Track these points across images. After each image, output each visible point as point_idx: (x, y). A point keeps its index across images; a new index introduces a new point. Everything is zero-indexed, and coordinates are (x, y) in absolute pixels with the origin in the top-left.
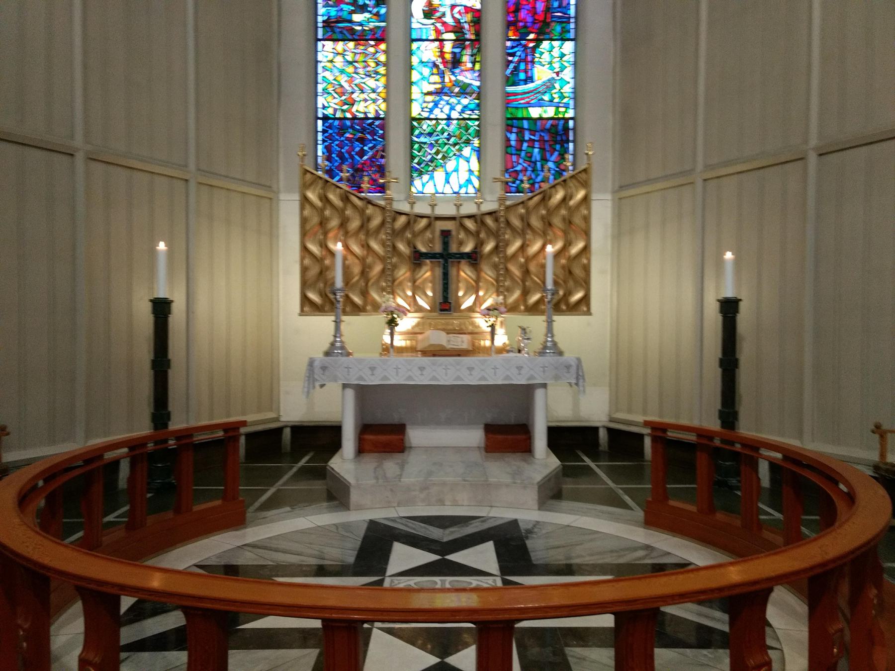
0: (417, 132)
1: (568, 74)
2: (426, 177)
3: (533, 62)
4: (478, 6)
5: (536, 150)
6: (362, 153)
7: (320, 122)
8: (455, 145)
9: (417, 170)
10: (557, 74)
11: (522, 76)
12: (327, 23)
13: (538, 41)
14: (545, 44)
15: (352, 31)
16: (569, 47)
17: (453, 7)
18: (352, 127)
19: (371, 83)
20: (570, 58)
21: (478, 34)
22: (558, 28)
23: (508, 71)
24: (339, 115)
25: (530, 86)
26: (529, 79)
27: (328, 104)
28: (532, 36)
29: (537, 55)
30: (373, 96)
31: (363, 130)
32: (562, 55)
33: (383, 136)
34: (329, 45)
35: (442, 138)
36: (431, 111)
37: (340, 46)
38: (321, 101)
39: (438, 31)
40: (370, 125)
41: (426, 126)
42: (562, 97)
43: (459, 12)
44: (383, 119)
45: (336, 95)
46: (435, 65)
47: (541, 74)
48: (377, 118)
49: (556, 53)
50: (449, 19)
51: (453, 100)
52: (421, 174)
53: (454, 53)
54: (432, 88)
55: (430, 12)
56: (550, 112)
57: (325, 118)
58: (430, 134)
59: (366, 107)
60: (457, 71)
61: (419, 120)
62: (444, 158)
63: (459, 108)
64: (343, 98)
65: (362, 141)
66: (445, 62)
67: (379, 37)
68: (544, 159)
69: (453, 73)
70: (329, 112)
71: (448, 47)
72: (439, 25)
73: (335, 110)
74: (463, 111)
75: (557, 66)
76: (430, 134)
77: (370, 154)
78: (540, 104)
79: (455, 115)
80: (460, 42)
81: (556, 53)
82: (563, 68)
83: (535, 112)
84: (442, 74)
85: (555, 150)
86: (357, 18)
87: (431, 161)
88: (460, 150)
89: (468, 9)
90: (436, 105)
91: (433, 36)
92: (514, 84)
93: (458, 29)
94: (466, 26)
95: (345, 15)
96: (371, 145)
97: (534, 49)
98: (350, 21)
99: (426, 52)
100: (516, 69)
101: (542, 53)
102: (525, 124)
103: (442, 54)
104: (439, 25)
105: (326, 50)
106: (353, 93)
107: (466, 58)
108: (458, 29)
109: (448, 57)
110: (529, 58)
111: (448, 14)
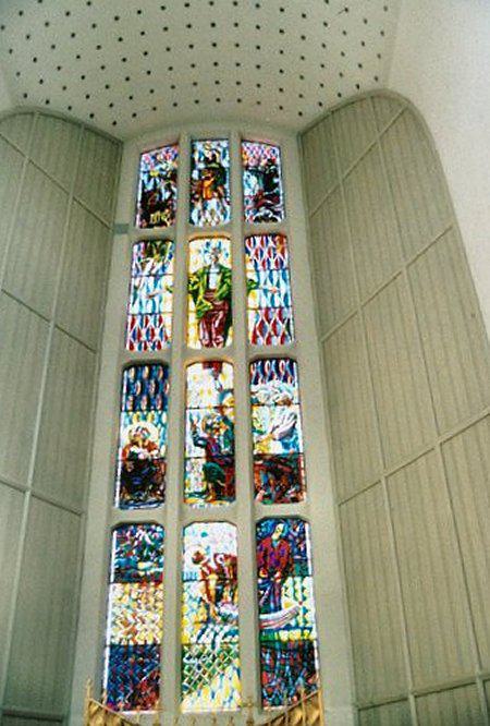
0: (187, 655)
1: (309, 604)
2: (195, 694)
3: (280, 594)
4: (235, 554)
5: (287, 668)
7: (108, 649)
8: (219, 664)
9: (187, 688)
10: (301, 603)
11: (272, 605)
12: (118, 571)
13: (284, 578)
14: (289, 580)
15: (138, 576)
17: (215, 556)
18: (134, 652)
19: (150, 616)
20: (309, 591)
21: (235, 575)
23: (262, 601)
24: (124, 643)
25: (279, 614)
26: (278, 608)
27: (114, 634)
28: (278, 575)
29: (283, 589)
30: (152, 626)
31: (143, 655)
33: (159, 660)
35: (209, 660)
36: (199, 638)
37: (128, 586)
38: (109, 632)
39: (203, 572)
40: (149, 651)
41: (195, 650)
42: (306, 622)
43: (221, 559)
44: (159, 645)
45: (121, 626)
46: (201, 599)
47: (288, 602)
48: (154, 644)
49: (298, 587)
51: (217, 628)
52: (190, 692)
53: (217, 591)
54: (201, 618)
55: (198, 559)
56: (295, 635)
57: (112, 646)
58: (198, 657)
59: (145, 637)
60: (220, 604)
61: (189, 645)
62: (210, 677)
63: (222, 634)
64: (128, 629)
65: (143, 665)
66: (209, 597)
67: (157, 579)
68: (295, 677)
69: (217, 605)
70: (116, 641)
71: (212, 584)
72: (205, 569)
73: (121, 640)
74: (225, 636)
75: (299, 595)
76: (198, 657)
77: (148, 675)
78: (288, 628)
79: (219, 640)
80: (222, 581)
81: (298, 587)
83: (284, 636)
84: (207, 607)
85: (303, 667)
86: (142, 565)
87: (200, 679)
88: (224, 669)
89: (227, 557)
90: (203, 631)
91: (200, 578)
92: (266, 613)
93: (220, 571)
94: (226, 569)
95: (132, 564)
96: (148, 667)
98: (137, 569)
99: (196, 590)
100: (267, 601)
101: (287, 588)
102: (277, 645)
103: (208, 592)
104: (205, 569)
105: (116, 591)
106: (136, 624)
107: (226, 594)
108: (220, 571)
109: (213, 593)
110: (277, 591)
111: (212, 561)
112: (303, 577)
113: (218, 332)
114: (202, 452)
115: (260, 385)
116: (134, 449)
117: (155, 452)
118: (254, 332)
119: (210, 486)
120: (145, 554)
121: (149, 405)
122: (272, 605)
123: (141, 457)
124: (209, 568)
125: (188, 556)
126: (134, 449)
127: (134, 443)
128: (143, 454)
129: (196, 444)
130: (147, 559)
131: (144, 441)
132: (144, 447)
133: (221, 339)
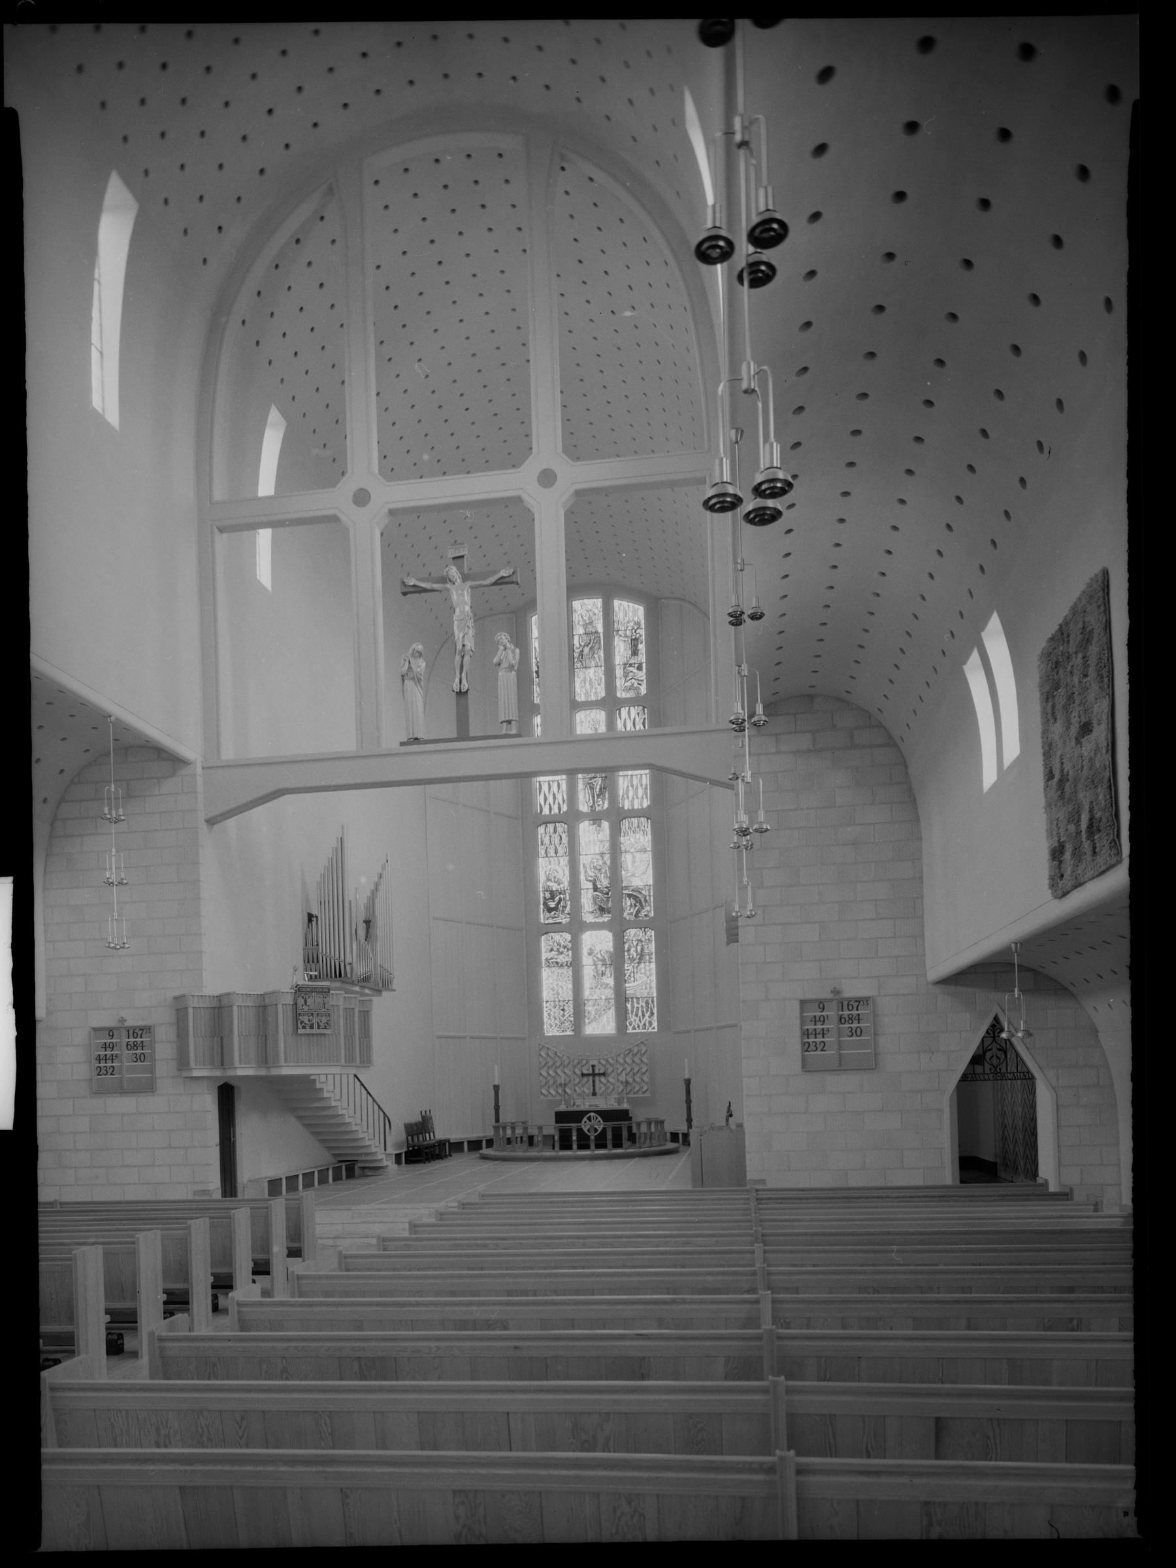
6: (564, 1015)
11: (632, 979)
12: (547, 960)
14: (642, 965)
15: (557, 963)
16: (653, 965)
17: (600, 951)
20: (654, 971)
22: (647, 957)
25: (636, 983)
34: (547, 969)
39: (594, 961)
49: (647, 968)
50: (600, 957)
66: (598, 975)
75: (648, 973)
81: (647, 968)
82: (651, 975)
89: (607, 951)
93: (604, 960)
97: (637, 967)
103: (597, 971)
108: (604, 960)
112: (650, 962)
113: (598, 796)
114: (590, 885)
115: (627, 838)
116: (548, 883)
117: (562, 886)
118: (623, 796)
119: (597, 907)
121: (556, 852)
122: (632, 979)
123: (554, 889)
125: (585, 951)
126: (548, 883)
127: (549, 880)
128: (555, 887)
129: (587, 880)
130: (562, 953)
131: (555, 878)
133: (601, 803)
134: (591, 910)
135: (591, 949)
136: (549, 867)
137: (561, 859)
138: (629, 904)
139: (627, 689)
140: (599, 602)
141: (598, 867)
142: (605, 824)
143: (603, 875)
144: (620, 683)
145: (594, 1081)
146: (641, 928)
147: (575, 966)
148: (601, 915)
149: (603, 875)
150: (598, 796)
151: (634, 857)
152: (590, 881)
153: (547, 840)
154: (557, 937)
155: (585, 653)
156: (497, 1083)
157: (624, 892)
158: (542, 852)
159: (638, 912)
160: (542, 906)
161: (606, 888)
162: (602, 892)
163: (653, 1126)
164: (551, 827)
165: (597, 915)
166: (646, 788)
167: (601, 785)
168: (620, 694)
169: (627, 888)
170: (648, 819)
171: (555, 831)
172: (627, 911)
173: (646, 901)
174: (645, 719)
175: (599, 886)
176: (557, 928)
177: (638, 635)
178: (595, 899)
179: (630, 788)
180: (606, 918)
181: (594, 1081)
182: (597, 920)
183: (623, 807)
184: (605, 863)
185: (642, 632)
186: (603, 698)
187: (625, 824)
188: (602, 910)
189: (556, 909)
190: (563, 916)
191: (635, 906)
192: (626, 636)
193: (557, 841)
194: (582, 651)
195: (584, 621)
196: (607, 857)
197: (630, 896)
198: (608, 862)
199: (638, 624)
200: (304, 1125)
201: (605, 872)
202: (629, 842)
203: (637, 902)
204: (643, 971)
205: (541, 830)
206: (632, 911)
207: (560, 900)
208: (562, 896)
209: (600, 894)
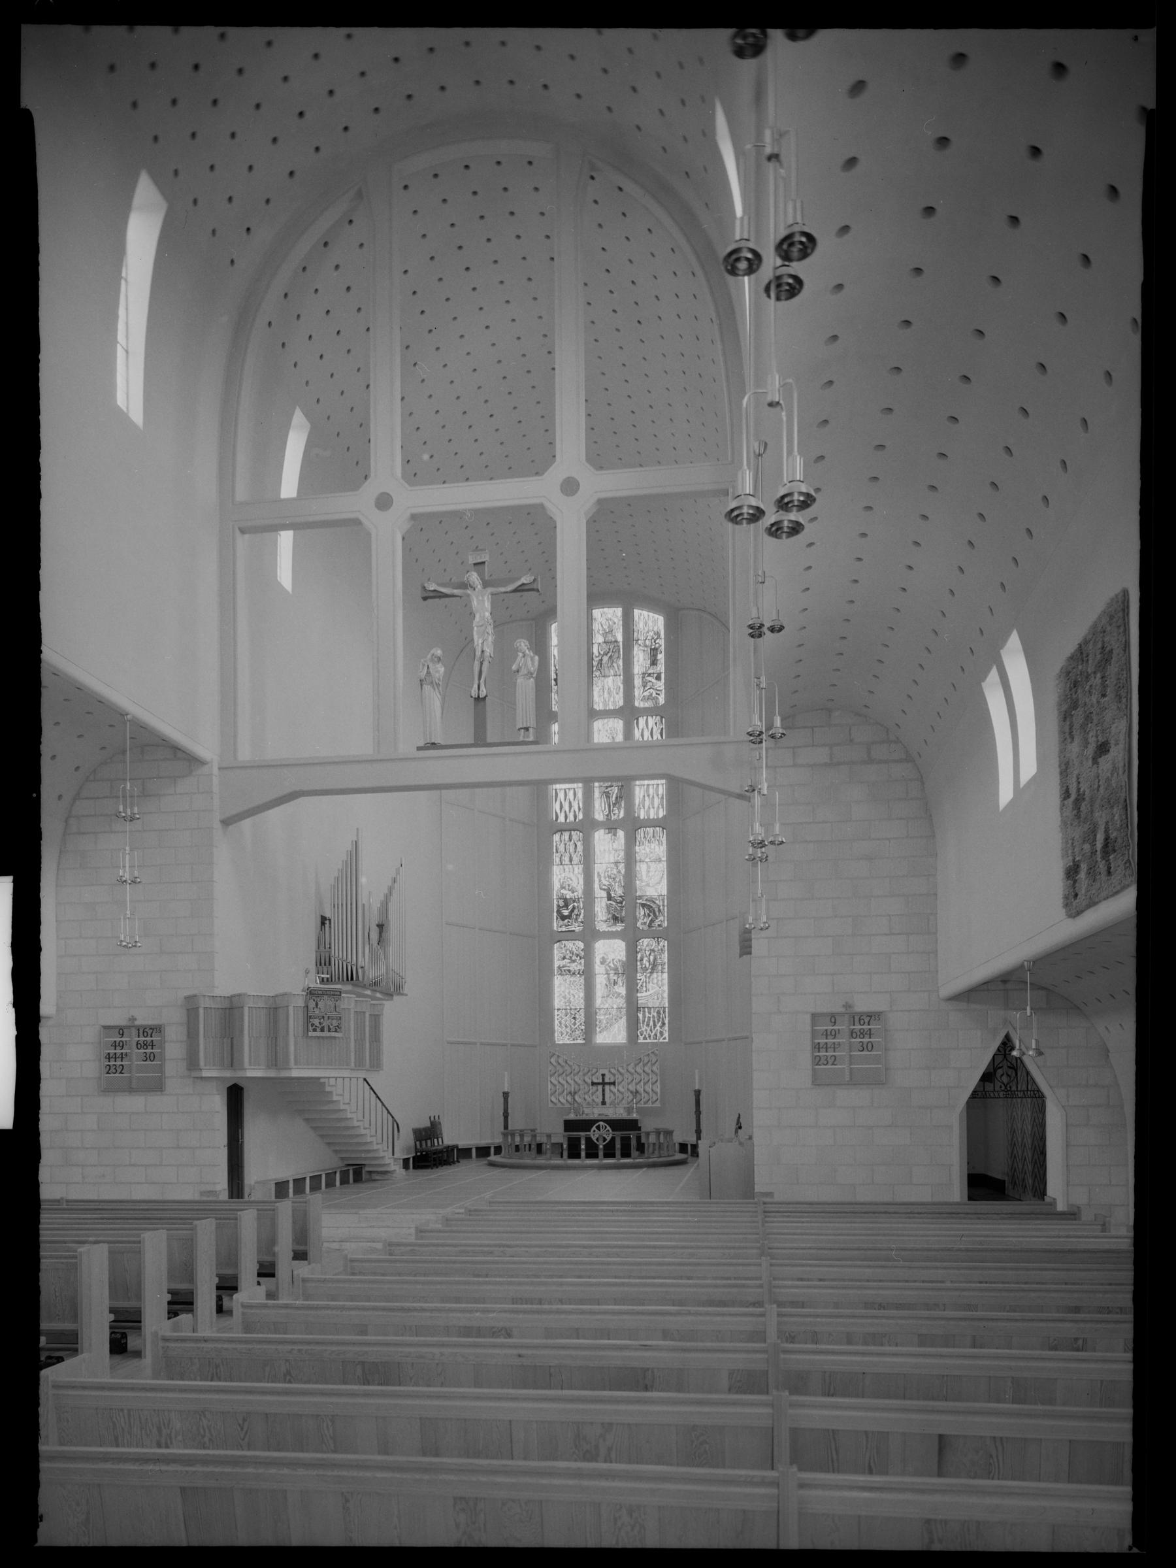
6: (575, 1024)
11: (644, 989)
12: (559, 967)
14: (655, 975)
15: (569, 971)
16: (666, 976)
17: (613, 960)
20: (666, 981)
22: (660, 968)
25: (648, 993)
32: (662, 979)
39: (606, 969)
49: (660, 978)
50: (611, 965)
55: (603, 962)
62: (611, 1025)
75: (660, 983)
81: (660, 978)
82: (663, 985)
89: (619, 961)
97: (649, 977)
113: (614, 805)
114: (604, 894)
116: (563, 891)
117: (576, 894)
118: (639, 805)
119: (610, 916)
120: (573, 958)
121: (571, 860)
122: (644, 989)
123: (568, 897)
124: (610, 967)
125: (597, 960)
126: (563, 891)
127: (563, 887)
128: (569, 895)
129: (601, 889)
130: (574, 961)
131: (569, 885)
132: (569, 890)
133: (617, 812)
134: (605, 918)
135: (603, 958)
136: (563, 875)
137: (576, 869)
138: (642, 913)
139: (645, 699)
140: (619, 611)
141: (613, 876)
142: (621, 834)
143: (617, 884)
144: (638, 692)
145: (603, 1090)
146: (654, 938)
147: (588, 974)
148: (615, 924)
149: (617, 884)
150: (614, 805)
151: (649, 867)
152: (604, 890)
153: (561, 848)
154: (569, 945)
155: (604, 662)
156: (506, 1090)
157: (638, 901)
158: (557, 859)
159: (652, 921)
160: (555, 914)
161: (621, 897)
162: (615, 901)
163: (662, 1136)
164: (566, 835)
165: (610, 924)
166: (662, 798)
167: (617, 794)
168: (638, 703)
169: (640, 897)
170: (663, 829)
171: (570, 840)
172: (641, 921)
173: (659, 911)
174: (662, 729)
175: (613, 895)
176: (570, 935)
177: (657, 645)
178: (608, 907)
179: (647, 798)
180: (619, 927)
181: (603, 1090)
182: (610, 929)
183: (639, 817)
184: (619, 872)
185: (662, 642)
186: (621, 708)
187: (640, 833)
188: (615, 919)
189: (569, 917)
190: (577, 924)
191: (649, 916)
192: (646, 646)
193: (572, 849)
194: (601, 660)
195: (604, 630)
196: (622, 867)
197: (643, 905)
198: (623, 871)
199: (658, 634)
200: (311, 1127)
201: (620, 881)
202: (643, 852)
203: (650, 912)
204: (655, 981)
205: (556, 837)
206: (645, 920)
207: (574, 908)
208: (575, 904)
209: (614, 903)
